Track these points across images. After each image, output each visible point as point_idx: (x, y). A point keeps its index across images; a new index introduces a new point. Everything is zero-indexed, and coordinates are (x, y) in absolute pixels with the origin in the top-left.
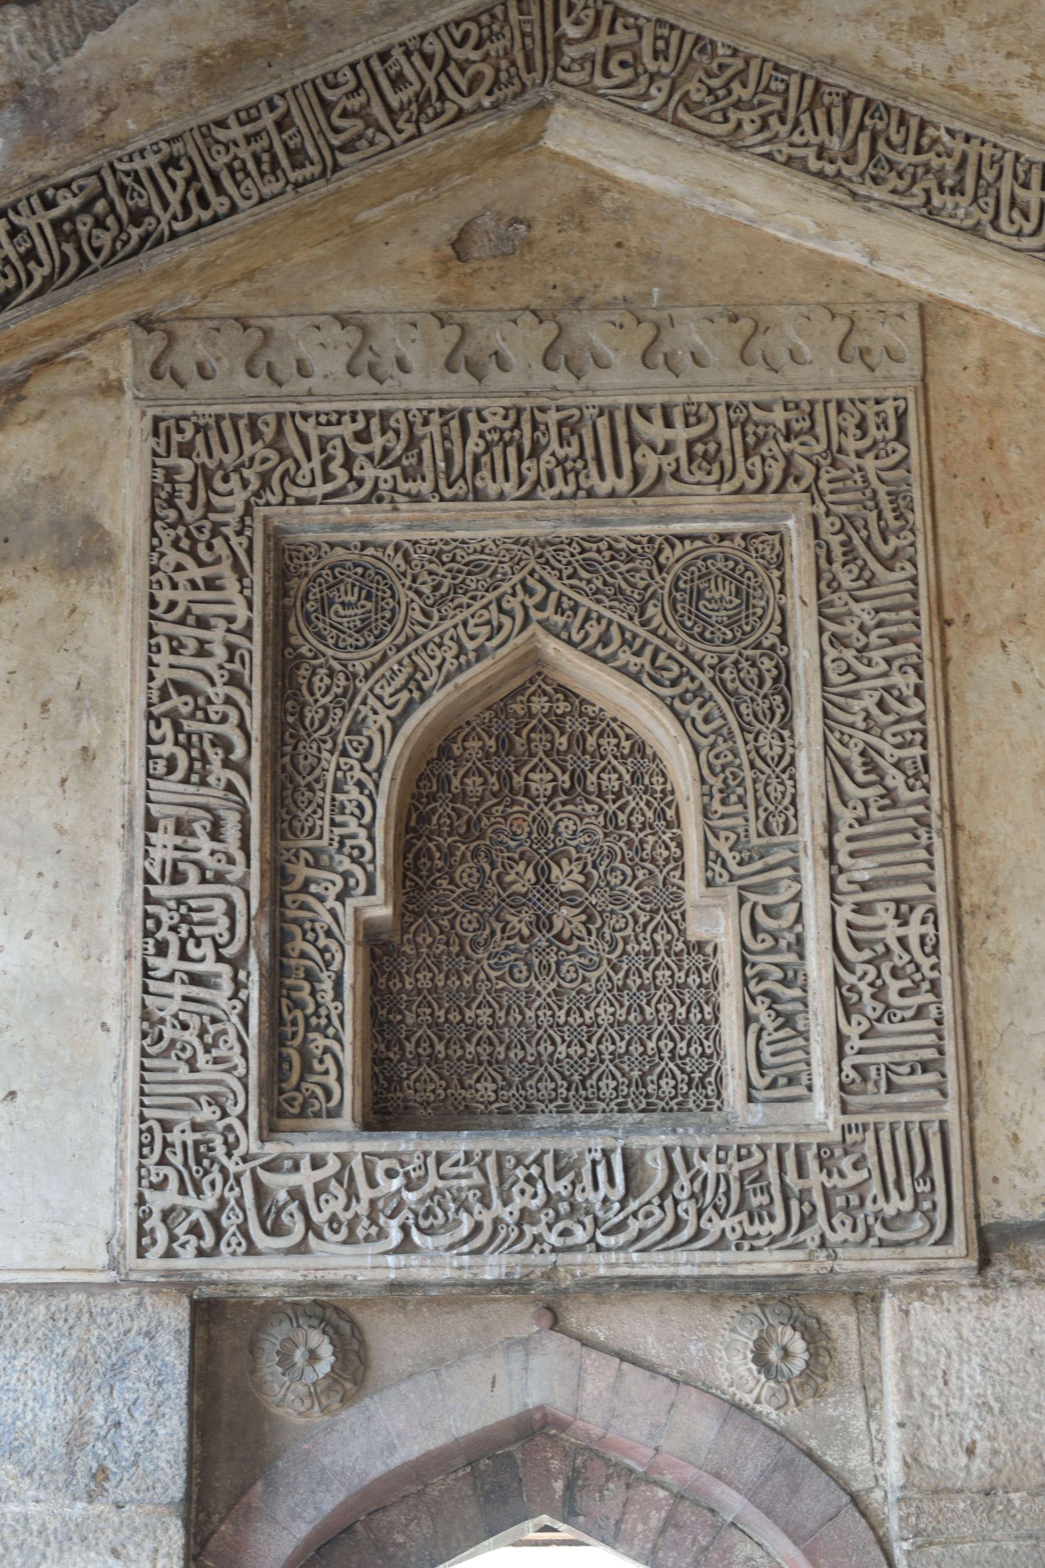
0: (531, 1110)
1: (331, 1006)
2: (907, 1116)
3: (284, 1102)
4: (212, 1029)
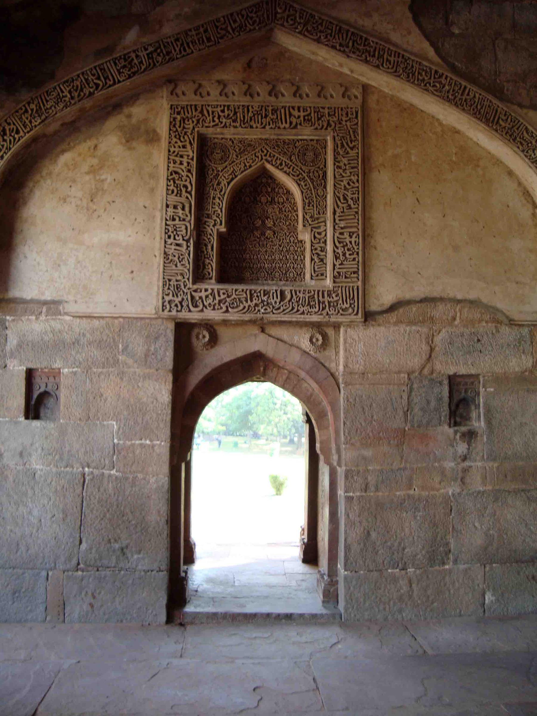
0: (258, 279)
3: (199, 276)
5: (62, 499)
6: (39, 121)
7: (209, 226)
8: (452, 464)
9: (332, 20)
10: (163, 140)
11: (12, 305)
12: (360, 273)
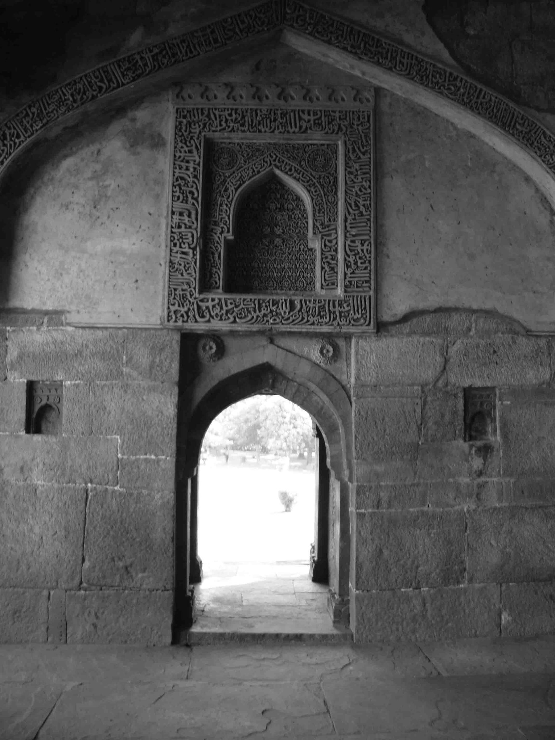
0: (267, 289)
2: (360, 294)
3: (206, 285)
5: (64, 515)
6: (41, 125)
7: (216, 234)
8: (467, 480)
9: (343, 21)
11: (13, 316)
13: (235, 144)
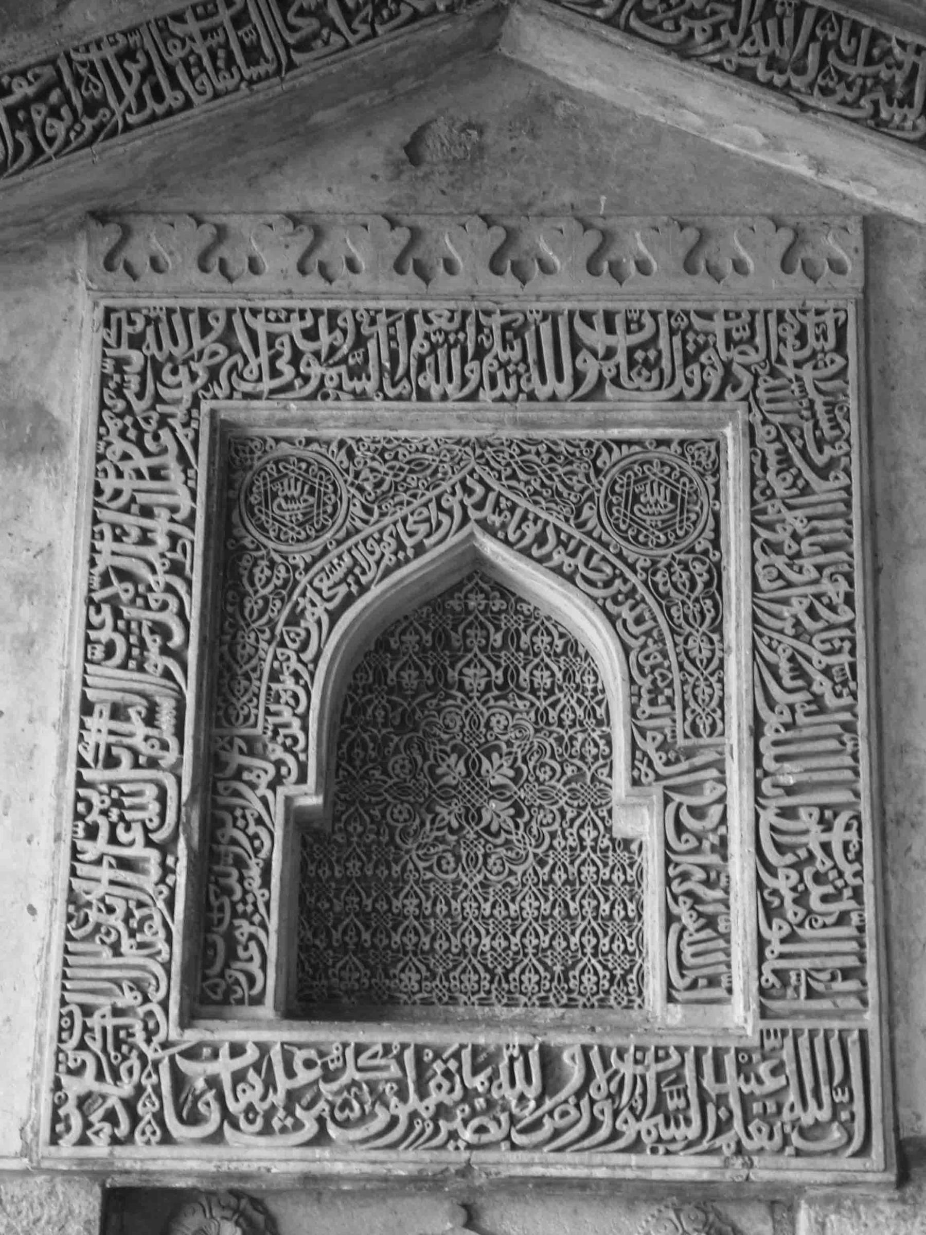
0: (453, 1000)
1: (258, 893)
3: (209, 988)
4: (138, 914)
7: (253, 786)
10: (73, 450)
12: (871, 975)
13: (328, 443)
